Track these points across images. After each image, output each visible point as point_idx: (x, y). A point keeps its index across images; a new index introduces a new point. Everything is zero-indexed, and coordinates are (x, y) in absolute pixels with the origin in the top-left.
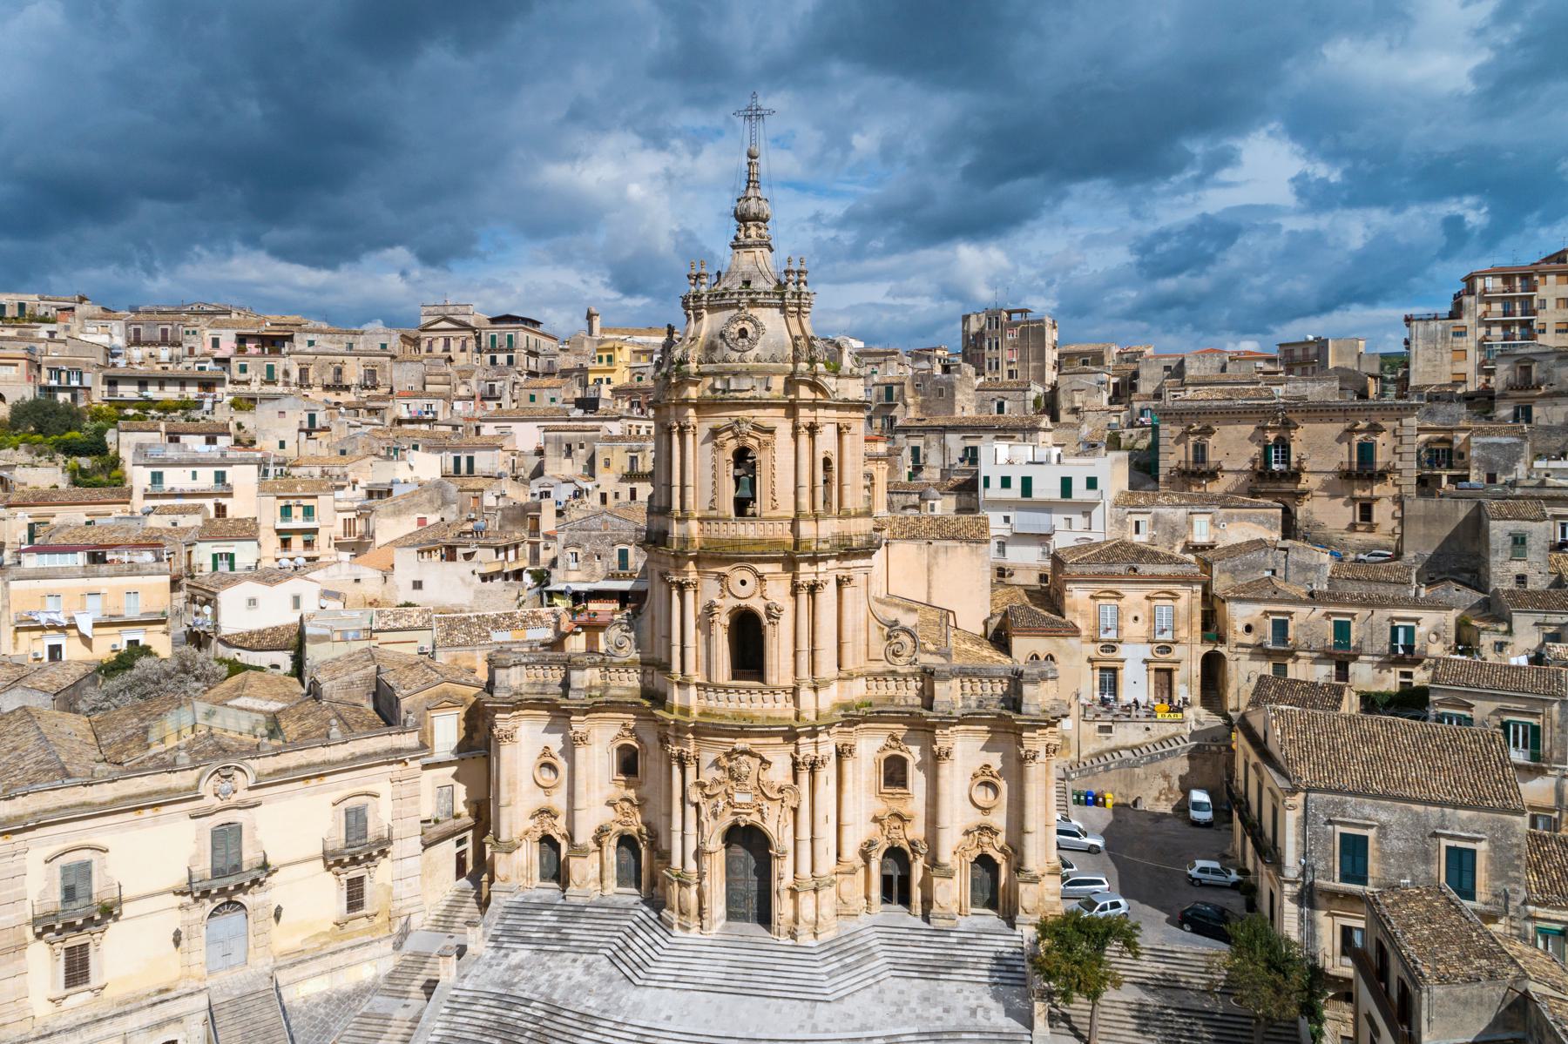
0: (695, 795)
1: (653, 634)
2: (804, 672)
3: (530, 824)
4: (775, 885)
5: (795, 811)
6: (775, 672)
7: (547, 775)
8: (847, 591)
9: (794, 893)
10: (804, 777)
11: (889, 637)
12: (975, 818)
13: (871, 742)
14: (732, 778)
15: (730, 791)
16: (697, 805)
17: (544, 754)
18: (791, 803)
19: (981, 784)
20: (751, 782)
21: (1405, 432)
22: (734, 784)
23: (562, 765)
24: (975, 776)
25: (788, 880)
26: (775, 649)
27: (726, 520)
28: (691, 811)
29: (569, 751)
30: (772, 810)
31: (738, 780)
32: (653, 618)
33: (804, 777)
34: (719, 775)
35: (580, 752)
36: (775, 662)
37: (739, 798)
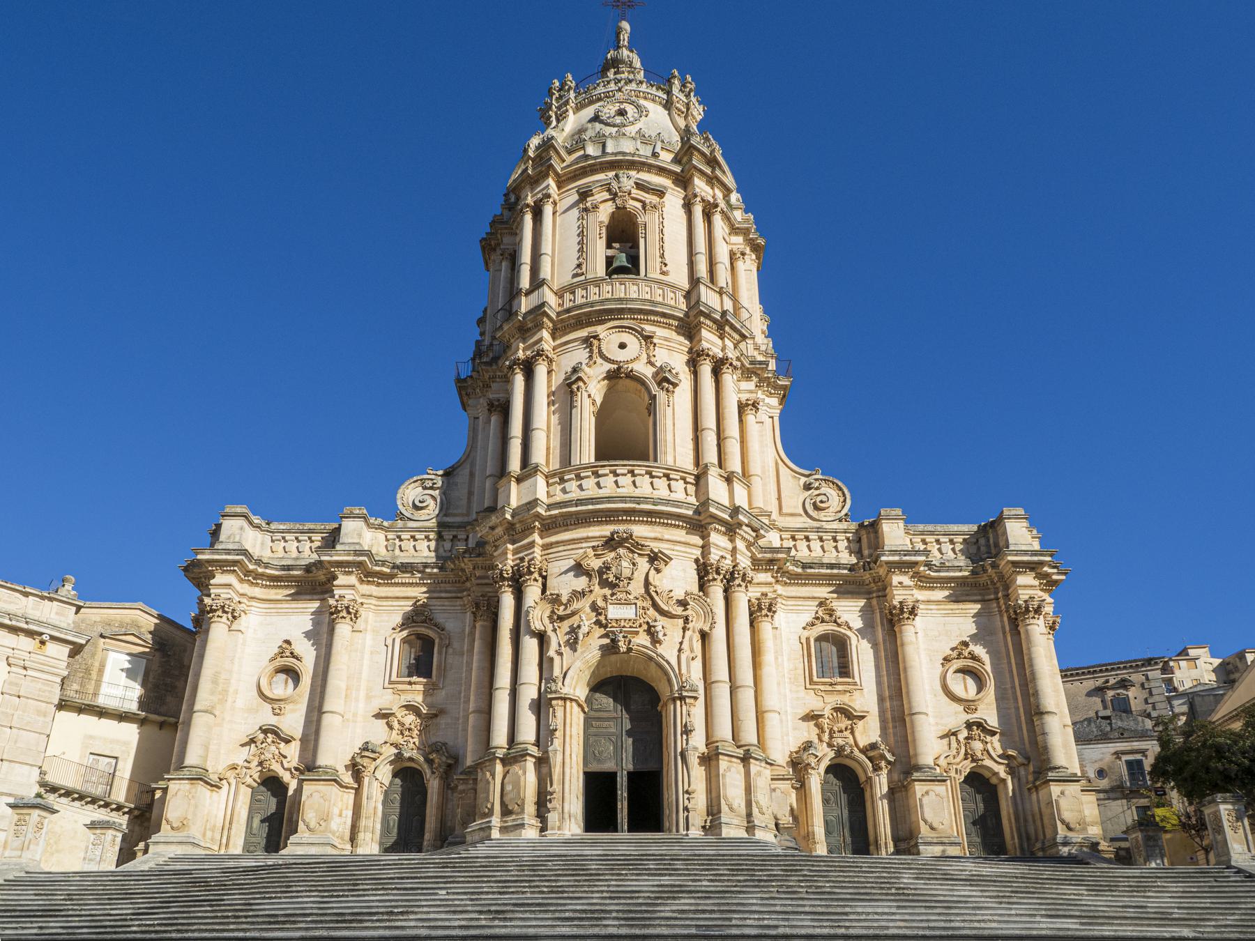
0: (538, 617)
1: (470, 493)
2: (711, 456)
3: (241, 756)
4: (674, 742)
5: (704, 636)
6: (670, 450)
7: (281, 688)
8: (750, 418)
9: (710, 759)
10: (717, 591)
11: (807, 487)
12: (956, 717)
13: (793, 616)
14: (604, 583)
15: (600, 603)
16: (542, 638)
17: (281, 653)
18: (697, 624)
19: (958, 671)
20: (637, 588)
21: (1153, 684)
22: (607, 592)
23: (307, 667)
24: (947, 660)
25: (698, 741)
26: (669, 422)
27: (597, 282)
28: (530, 646)
29: (322, 634)
30: (671, 632)
31: (613, 586)
32: (472, 475)
33: (717, 591)
34: (581, 583)
35: (343, 629)
36: (669, 437)
37: (614, 612)
